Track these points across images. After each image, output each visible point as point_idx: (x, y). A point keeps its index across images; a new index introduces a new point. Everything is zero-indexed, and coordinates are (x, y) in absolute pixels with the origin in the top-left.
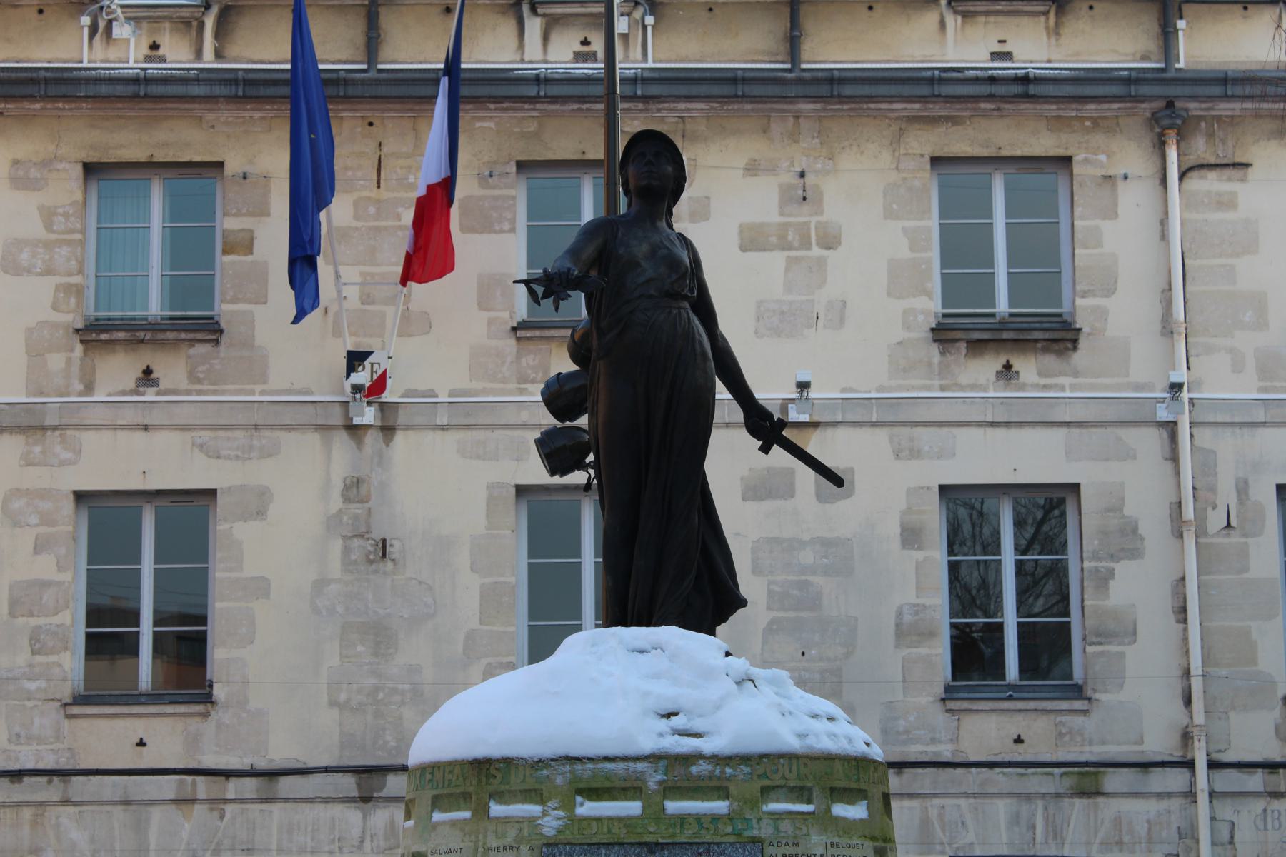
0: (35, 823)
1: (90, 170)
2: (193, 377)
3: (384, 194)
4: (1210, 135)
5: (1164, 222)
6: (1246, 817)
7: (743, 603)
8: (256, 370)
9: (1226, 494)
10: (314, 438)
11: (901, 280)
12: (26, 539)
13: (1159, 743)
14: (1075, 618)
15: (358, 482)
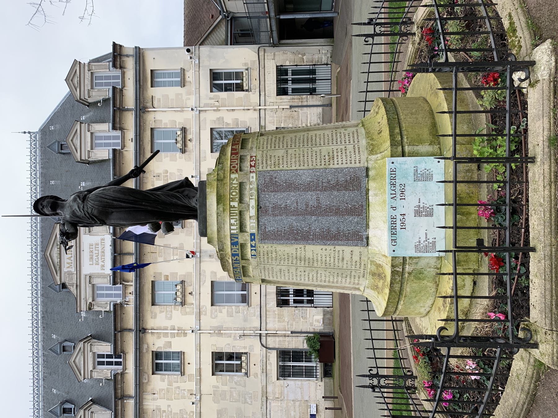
0: (269, 312)
1: (153, 304)
2: (191, 285)
3: (157, 252)
4: (147, 103)
5: (163, 111)
6: (269, 100)
7: (187, 179)
8: (189, 274)
9: (212, 102)
10: (202, 264)
11: (173, 159)
12: (219, 314)
13: (256, 114)
14: (235, 130)
15: (210, 256)
